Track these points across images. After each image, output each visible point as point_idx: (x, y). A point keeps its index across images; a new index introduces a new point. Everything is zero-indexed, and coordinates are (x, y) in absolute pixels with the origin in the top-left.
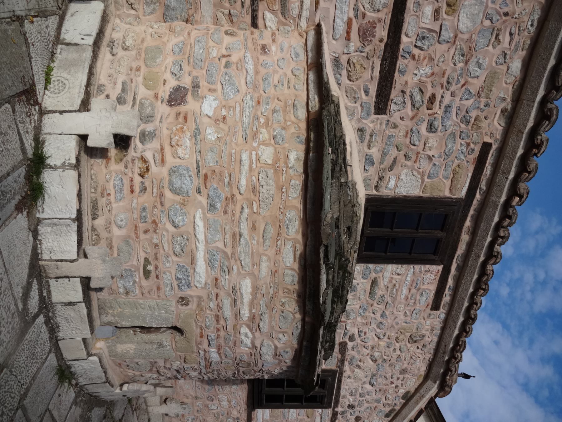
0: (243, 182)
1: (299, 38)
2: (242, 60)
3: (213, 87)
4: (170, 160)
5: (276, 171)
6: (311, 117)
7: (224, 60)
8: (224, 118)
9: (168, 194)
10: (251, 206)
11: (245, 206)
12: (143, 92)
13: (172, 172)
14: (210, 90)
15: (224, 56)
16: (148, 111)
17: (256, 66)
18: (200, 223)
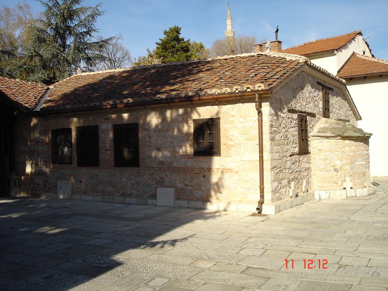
0: (352, 154)
1: (314, 141)
2: (325, 156)
3: (333, 162)
4: (349, 171)
5: (350, 146)
6: (341, 138)
7: (325, 160)
8: (341, 159)
9: (355, 170)
10: (355, 152)
11: (355, 153)
12: (335, 179)
13: (351, 170)
14: (334, 163)
15: (323, 160)
16: (340, 176)
17: (326, 152)
18: (358, 163)
